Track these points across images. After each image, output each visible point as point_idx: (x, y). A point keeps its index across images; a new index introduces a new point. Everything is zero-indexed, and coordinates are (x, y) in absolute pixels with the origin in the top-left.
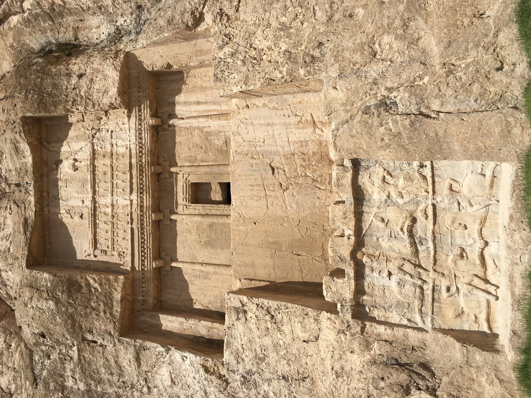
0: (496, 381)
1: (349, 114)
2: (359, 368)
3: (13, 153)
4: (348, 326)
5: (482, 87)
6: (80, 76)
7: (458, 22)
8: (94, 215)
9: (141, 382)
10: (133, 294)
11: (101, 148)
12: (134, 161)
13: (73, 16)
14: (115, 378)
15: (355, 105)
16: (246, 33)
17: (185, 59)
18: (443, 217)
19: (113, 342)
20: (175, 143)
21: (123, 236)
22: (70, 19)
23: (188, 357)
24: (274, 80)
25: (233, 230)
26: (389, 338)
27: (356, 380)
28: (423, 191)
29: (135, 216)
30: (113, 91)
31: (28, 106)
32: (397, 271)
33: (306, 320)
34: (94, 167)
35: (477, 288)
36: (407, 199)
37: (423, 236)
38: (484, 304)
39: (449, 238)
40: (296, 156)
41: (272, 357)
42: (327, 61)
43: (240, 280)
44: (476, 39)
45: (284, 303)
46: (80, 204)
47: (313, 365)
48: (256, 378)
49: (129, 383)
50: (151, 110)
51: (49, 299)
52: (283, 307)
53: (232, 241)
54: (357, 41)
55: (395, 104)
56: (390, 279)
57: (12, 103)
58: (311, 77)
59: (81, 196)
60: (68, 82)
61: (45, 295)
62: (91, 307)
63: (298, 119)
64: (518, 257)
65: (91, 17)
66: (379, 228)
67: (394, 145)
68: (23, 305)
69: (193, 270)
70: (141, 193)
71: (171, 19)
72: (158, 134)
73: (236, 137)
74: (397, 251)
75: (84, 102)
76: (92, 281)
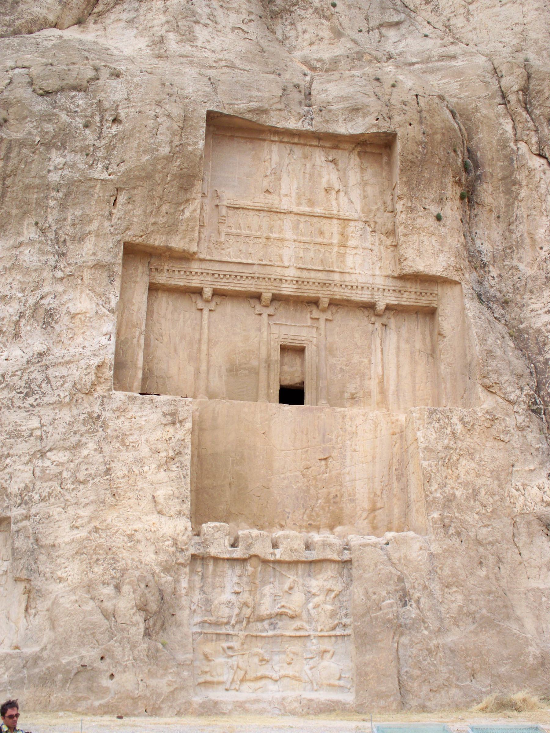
0: (172, 689)
1: (396, 561)
3: (350, 103)
4: (182, 550)
5: (418, 677)
6: (438, 218)
9: (69, 269)
11: (353, 232)
12: (336, 277)
13: (505, 207)
15: (405, 568)
16: (474, 449)
19: (117, 232)
21: (244, 251)
22: (502, 202)
23: (109, 342)
28: (322, 627)
32: (242, 600)
33: (176, 501)
36: (313, 612)
37: (278, 626)
38: (221, 679)
40: (339, 488)
41: (128, 456)
44: (455, 672)
45: (189, 473)
51: (172, 147)
52: (185, 473)
55: (405, 605)
57: (413, 119)
58: (431, 524)
59: (294, 195)
60: (433, 201)
61: (176, 142)
62: (161, 205)
63: (378, 493)
64: (276, 706)
65: (501, 232)
67: (369, 604)
68: (158, 98)
69: (200, 340)
70: (297, 281)
71: (493, 354)
73: (361, 417)
74: (262, 602)
75: (409, 222)
76: (191, 207)
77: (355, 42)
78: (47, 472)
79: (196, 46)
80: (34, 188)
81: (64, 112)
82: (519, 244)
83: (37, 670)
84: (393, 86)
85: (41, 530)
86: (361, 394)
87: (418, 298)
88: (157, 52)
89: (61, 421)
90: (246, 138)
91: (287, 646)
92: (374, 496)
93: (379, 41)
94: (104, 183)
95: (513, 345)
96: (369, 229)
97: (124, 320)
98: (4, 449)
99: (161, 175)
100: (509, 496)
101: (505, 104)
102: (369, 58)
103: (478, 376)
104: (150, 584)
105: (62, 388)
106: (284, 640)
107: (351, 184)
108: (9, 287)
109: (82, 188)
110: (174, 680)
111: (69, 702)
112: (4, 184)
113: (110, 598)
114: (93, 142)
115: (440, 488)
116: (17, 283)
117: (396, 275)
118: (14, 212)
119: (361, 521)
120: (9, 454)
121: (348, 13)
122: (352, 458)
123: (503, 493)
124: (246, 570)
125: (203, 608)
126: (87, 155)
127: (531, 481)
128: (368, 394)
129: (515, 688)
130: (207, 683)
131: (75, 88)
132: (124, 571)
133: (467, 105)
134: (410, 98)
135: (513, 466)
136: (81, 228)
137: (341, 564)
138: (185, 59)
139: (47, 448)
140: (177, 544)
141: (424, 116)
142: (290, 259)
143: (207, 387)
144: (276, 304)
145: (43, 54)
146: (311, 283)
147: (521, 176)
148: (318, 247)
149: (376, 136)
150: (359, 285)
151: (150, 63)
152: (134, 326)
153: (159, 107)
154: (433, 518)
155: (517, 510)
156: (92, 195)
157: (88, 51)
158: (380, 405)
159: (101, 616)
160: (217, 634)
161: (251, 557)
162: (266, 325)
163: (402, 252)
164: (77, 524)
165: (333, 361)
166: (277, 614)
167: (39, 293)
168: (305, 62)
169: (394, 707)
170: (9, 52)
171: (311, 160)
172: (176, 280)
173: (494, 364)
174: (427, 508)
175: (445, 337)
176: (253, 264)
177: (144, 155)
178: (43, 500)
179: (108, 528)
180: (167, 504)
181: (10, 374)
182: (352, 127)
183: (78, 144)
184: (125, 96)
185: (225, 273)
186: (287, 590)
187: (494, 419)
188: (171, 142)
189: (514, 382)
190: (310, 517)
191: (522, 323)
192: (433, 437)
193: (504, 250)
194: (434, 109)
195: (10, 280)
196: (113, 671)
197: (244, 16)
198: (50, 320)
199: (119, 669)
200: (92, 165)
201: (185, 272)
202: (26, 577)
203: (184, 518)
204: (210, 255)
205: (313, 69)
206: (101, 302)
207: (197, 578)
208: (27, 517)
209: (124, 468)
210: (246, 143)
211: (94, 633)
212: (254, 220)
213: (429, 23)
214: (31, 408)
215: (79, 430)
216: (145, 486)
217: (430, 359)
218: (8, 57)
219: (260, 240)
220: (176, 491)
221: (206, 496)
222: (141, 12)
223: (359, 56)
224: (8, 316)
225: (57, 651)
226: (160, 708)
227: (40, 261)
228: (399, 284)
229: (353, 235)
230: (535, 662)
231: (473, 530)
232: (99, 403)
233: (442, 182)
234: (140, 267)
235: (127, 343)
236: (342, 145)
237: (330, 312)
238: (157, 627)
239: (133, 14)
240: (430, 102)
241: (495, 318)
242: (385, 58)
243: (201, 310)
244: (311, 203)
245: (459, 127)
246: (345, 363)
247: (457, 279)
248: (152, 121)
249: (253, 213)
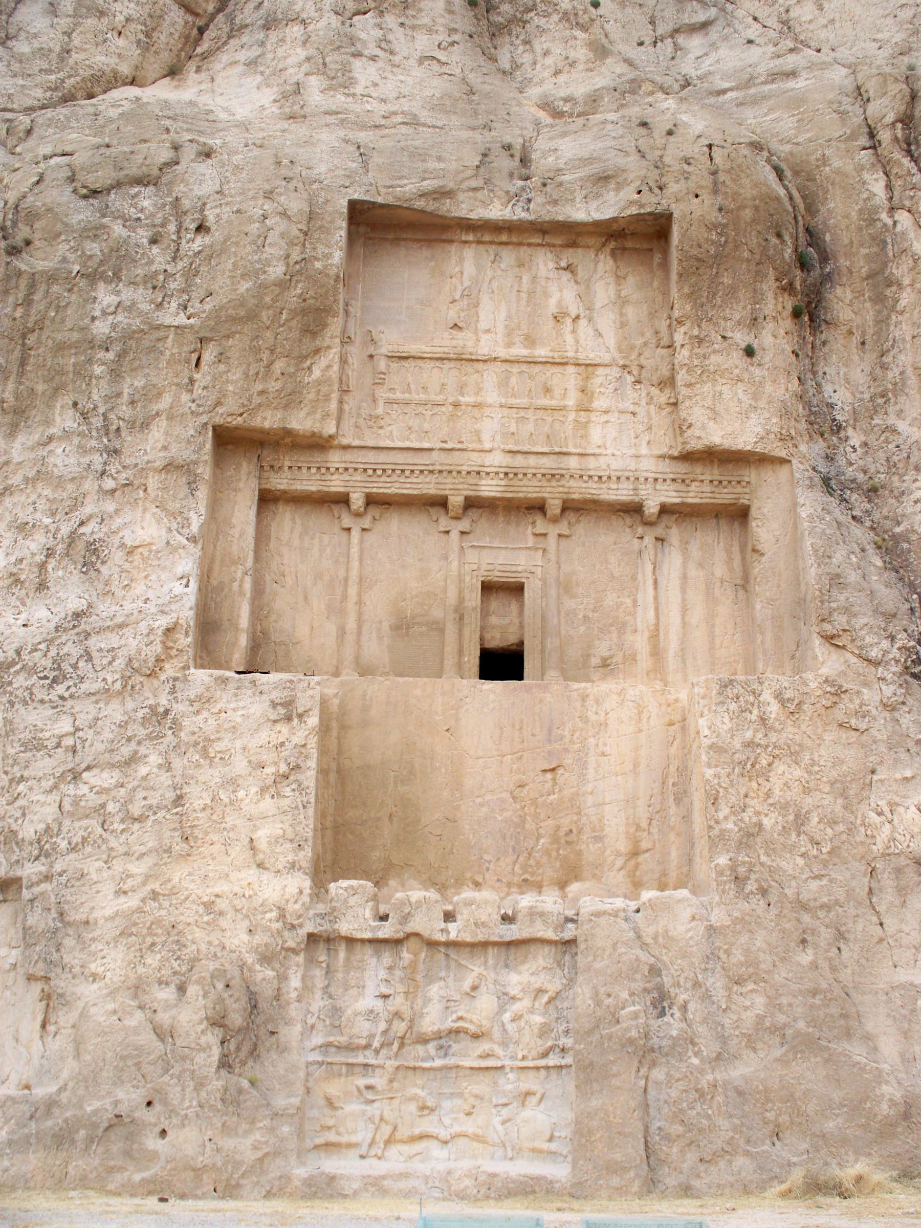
0: (260, 1154)
1: (649, 940)
3: (595, 169)
4: (293, 927)
5: (678, 1136)
6: (749, 352)
9: (124, 475)
11: (601, 385)
12: (573, 463)
15: (664, 951)
16: (800, 745)
17: (768, 594)
19: (201, 409)
22: (870, 317)
23: (187, 590)
28: (525, 1052)
31: (694, 232)
33: (288, 845)
36: (510, 1027)
37: (451, 1051)
38: (353, 1139)
39: (451, 1091)
40: (575, 818)
41: (212, 775)
43: (336, 695)
44: (745, 1129)
45: (313, 800)
51: (288, 264)
52: (305, 799)
53: (411, 679)
54: (761, 954)
55: (662, 1014)
57: (702, 187)
59: (500, 329)
61: (296, 256)
62: (272, 362)
63: (644, 825)
64: (437, 1184)
65: (868, 369)
67: (599, 1014)
68: (267, 187)
69: (346, 580)
70: (506, 474)
73: (615, 697)
74: (425, 1011)
76: (323, 362)
77: (629, 62)
78: (83, 804)
79: (354, 95)
80: (70, 347)
81: (119, 221)
82: (899, 388)
83: (49, 1123)
84: (670, 133)
85: (69, 898)
86: (619, 658)
87: (716, 490)
88: (287, 110)
90: (419, 241)
91: (465, 1084)
92: (636, 830)
93: (673, 58)
94: (179, 331)
95: (879, 563)
96: (630, 379)
97: (218, 553)
98: (16, 768)
99: (271, 312)
100: (863, 824)
101: (874, 147)
102: (651, 89)
103: (813, 619)
104: (232, 983)
105: (111, 668)
106: (461, 1074)
107: (598, 305)
108: (31, 509)
109: (146, 343)
111: (95, 1174)
112: (24, 344)
113: (168, 1007)
114: (163, 267)
115: (733, 813)
116: (44, 501)
117: (676, 454)
119: (612, 874)
120: (22, 776)
121: (620, 16)
122: (599, 766)
123: (852, 819)
124: (400, 958)
126: (154, 288)
127: (905, 797)
128: (632, 658)
129: (852, 1157)
130: (329, 1146)
131: (139, 181)
132: (193, 962)
133: (808, 155)
134: (697, 151)
135: (873, 772)
136: (144, 407)
137: (560, 946)
138: (334, 117)
139: (84, 766)
140: (284, 916)
141: (721, 180)
142: (494, 436)
143: (357, 658)
144: (473, 513)
145: (99, 131)
146: (529, 476)
147: (901, 270)
148: (541, 414)
149: (638, 220)
150: (613, 473)
151: (275, 128)
152: (234, 562)
153: (270, 202)
154: (718, 864)
155: (878, 847)
156: (161, 353)
157: (174, 118)
158: (652, 676)
159: (153, 1036)
160: (347, 1064)
161: (409, 936)
162: (456, 549)
163: (683, 414)
164: (125, 887)
165: (569, 604)
166: (450, 1032)
167: (76, 517)
168: (546, 105)
169: (635, 1188)
170: (51, 131)
171: (530, 268)
172: (305, 483)
173: (841, 598)
174: (710, 848)
175: (762, 555)
176: (431, 450)
177: (242, 282)
178: (73, 849)
179: (172, 893)
180: (273, 852)
181: (29, 648)
182: (597, 209)
183: (139, 271)
184: (218, 188)
185: (384, 467)
186: (468, 990)
187: (840, 692)
188: (288, 256)
189: (879, 627)
190: (525, 868)
191: (898, 524)
192: (725, 727)
193: (872, 399)
194: (739, 166)
195: (33, 497)
196: (165, 1124)
197: (442, 37)
198: (94, 559)
199: (175, 1121)
200: (161, 304)
201: (319, 468)
202: (42, 974)
203: (300, 873)
204: (359, 438)
205: (557, 114)
206: (174, 526)
207: (318, 973)
208: (47, 878)
209: (205, 795)
210: (420, 248)
211: (140, 1063)
212: (433, 375)
213: (755, 19)
214: (60, 702)
215: (135, 735)
216: (238, 822)
217: (741, 592)
218: (47, 140)
219: (443, 409)
220: (289, 831)
221: (350, 837)
222: (269, 47)
223: (634, 86)
224: (29, 556)
225: (81, 1092)
226: (238, 1186)
227: (79, 464)
228: (682, 468)
229: (602, 390)
230: (892, 1113)
232: (168, 690)
233: (755, 291)
234: (245, 464)
235: (223, 589)
236: (582, 241)
237: (565, 523)
238: (243, 1054)
239: (255, 52)
240: (733, 155)
241: (854, 518)
242: (676, 87)
243: (349, 529)
244: (530, 341)
245: (789, 193)
246: (592, 607)
247: (783, 454)
248: (257, 225)
249: (432, 364)
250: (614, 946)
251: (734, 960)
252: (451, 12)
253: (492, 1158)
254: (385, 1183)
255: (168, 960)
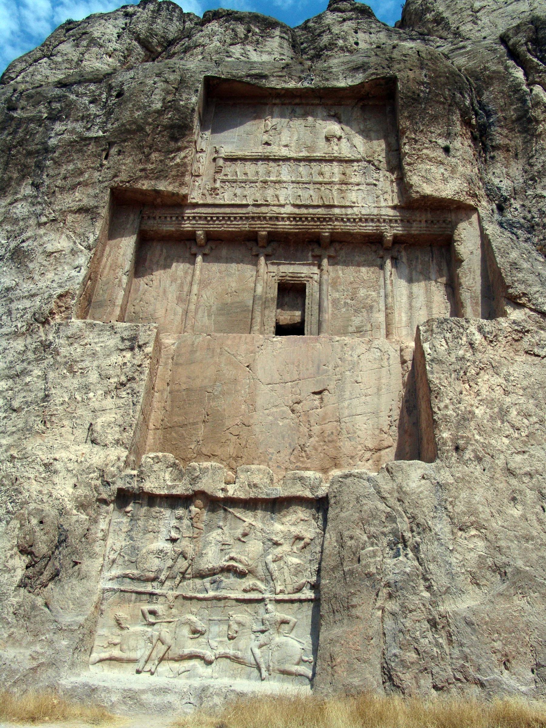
2: (55, 493)
3: (351, 65)
4: (108, 483)
5: (412, 663)
6: (447, 150)
7: (496, 635)
8: (266, 159)
10: (164, 205)
11: (355, 171)
12: (337, 211)
14: (59, 183)
16: (498, 362)
18: (247, 611)
20: (359, 265)
21: (238, 194)
22: (519, 141)
24: (436, 397)
25: (241, 338)
26: (92, 534)
27: (41, 489)
28: (282, 588)
29: (264, 209)
30: (428, 190)
33: (117, 429)
34: (331, 161)
35: (153, 648)
36: (273, 566)
37: (223, 585)
38: (132, 655)
39: (219, 618)
40: (335, 423)
41: (73, 383)
42: (458, 467)
43: (173, 344)
45: (141, 400)
46: (284, 143)
47: (61, 435)
48: (48, 360)
49: (53, 200)
50: (402, 235)
51: (164, 103)
52: (135, 400)
53: (225, 334)
56: (167, 540)
60: (439, 135)
61: (169, 98)
62: (150, 154)
64: (192, 701)
65: (520, 167)
66: (235, 529)
68: (158, 72)
72: (371, 243)
74: (204, 552)
75: (414, 152)
89: (12, 351)
110: (43, 651)
118: (16, 175)
125: (126, 558)
140: (103, 476)
144: (274, 245)
182: (352, 81)
186: (240, 536)
190: (298, 458)
193: (524, 182)
215: (28, 359)
219: (257, 184)
231: (502, 456)
250: (357, 499)
251: (457, 510)
252: (282, 48)
253: (249, 678)
254: (144, 697)
255: (5, 503)
